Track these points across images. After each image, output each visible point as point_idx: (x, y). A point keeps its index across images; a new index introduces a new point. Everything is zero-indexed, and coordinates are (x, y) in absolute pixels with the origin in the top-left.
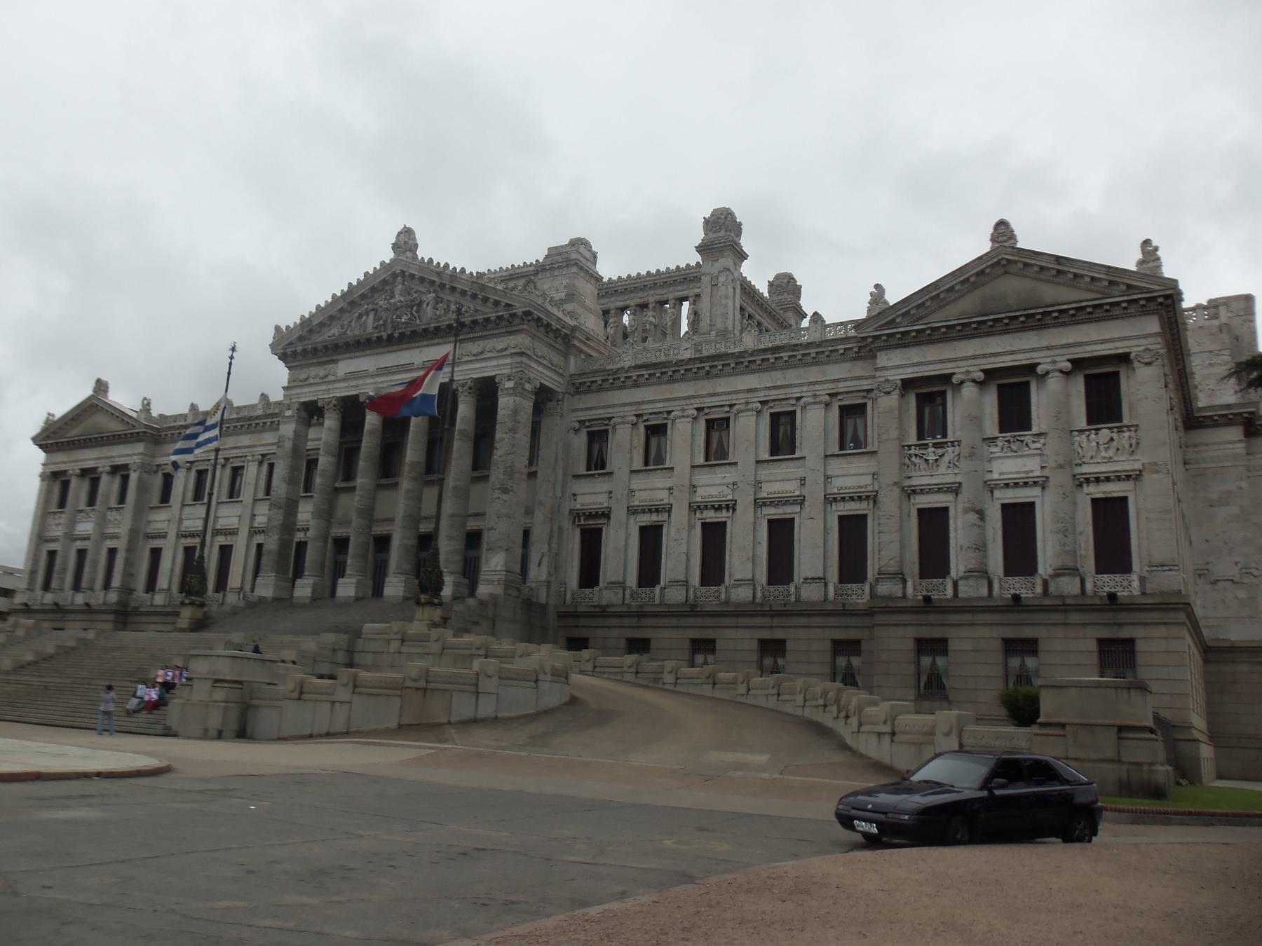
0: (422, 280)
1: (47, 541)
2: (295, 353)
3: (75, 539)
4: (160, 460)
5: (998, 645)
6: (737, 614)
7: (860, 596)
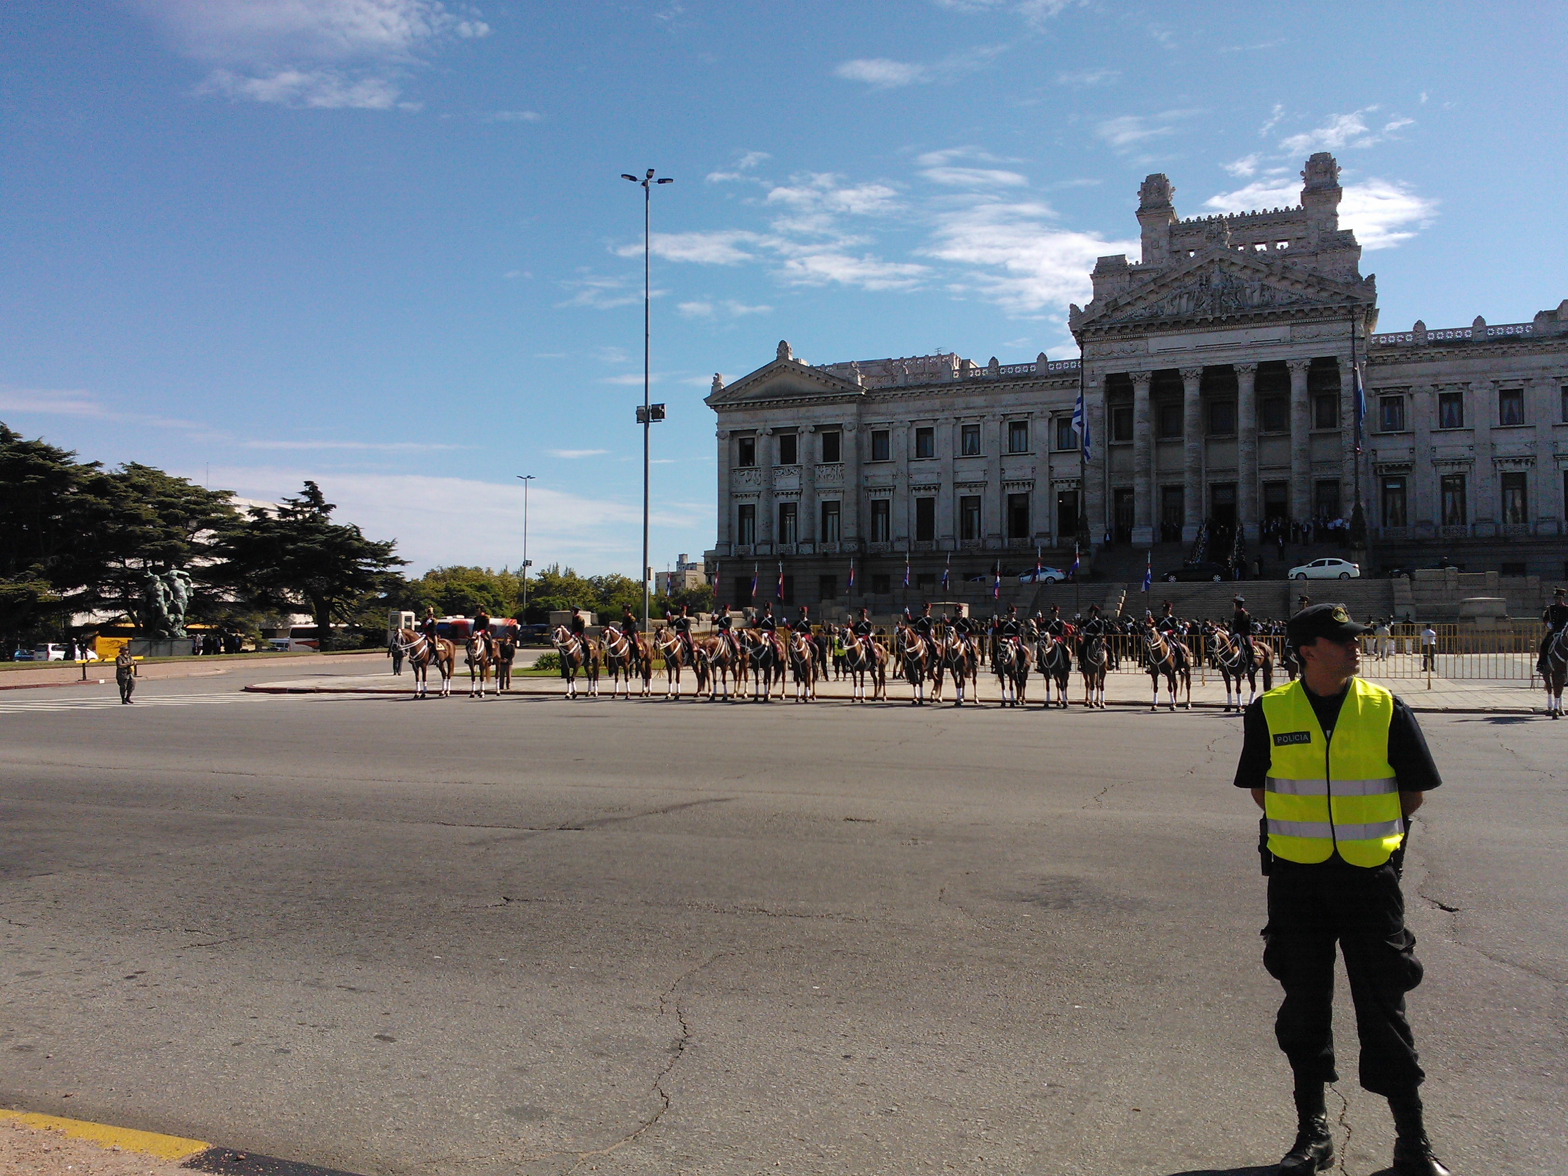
0: (1245, 267)
1: (737, 496)
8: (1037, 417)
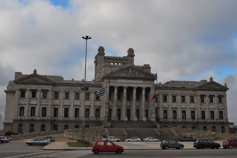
0: (136, 69)
1: (20, 104)
3: (30, 105)
4: (54, 89)
5: (212, 127)
6: (180, 123)
7: (195, 121)
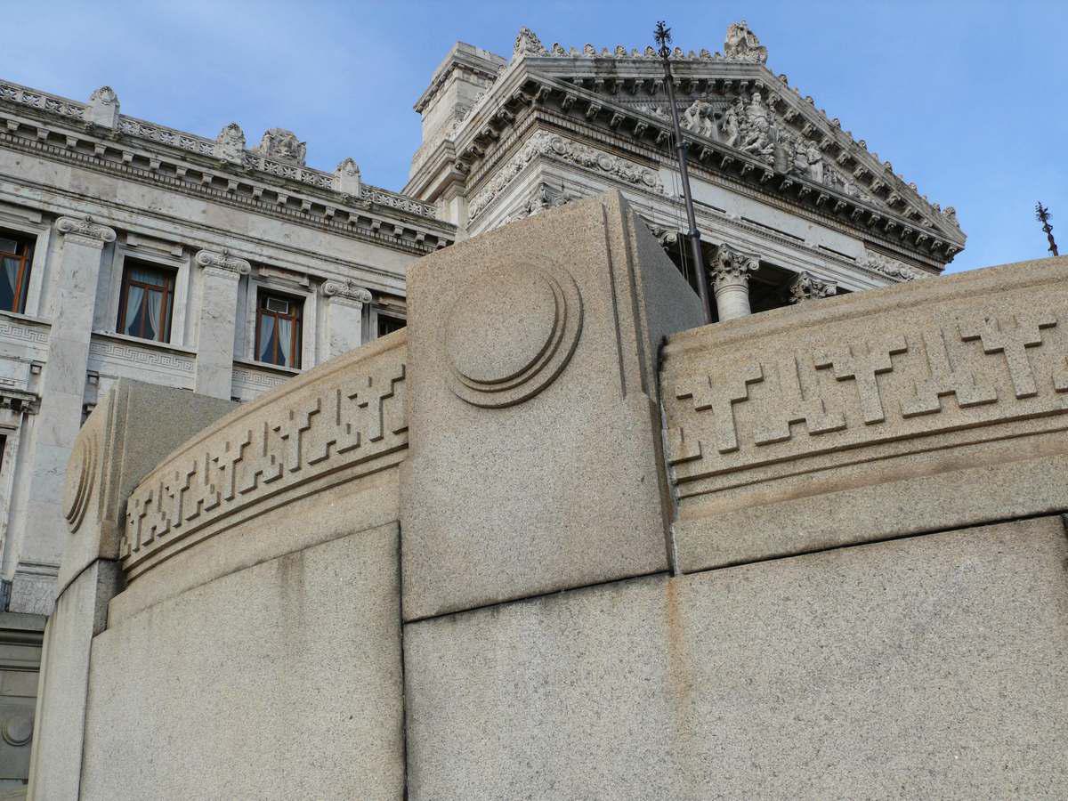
0: (797, 121)
2: (581, 105)
8: (336, 293)
